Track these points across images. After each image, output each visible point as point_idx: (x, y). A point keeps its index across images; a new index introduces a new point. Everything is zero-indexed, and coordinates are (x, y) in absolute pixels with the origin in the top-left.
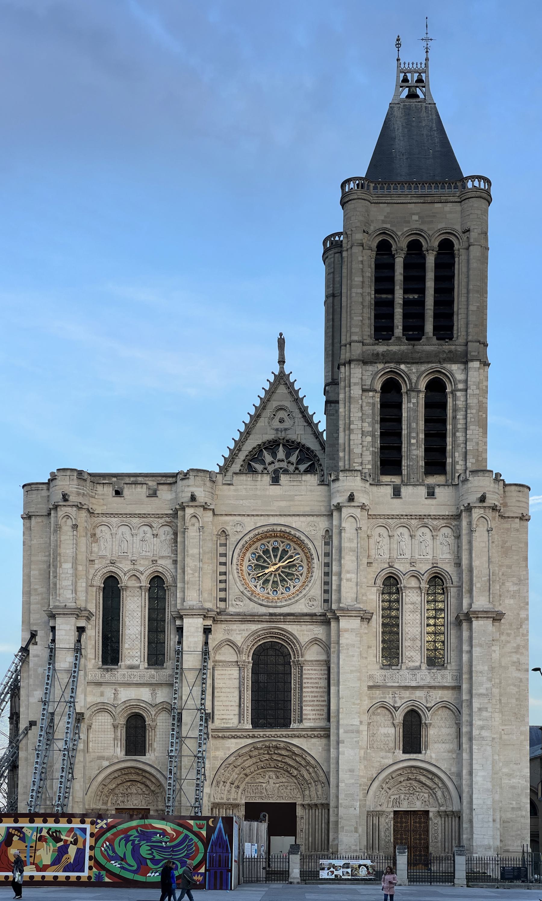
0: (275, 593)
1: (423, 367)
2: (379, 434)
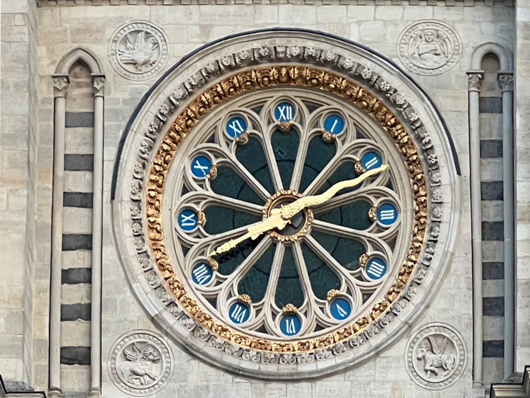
0: (291, 324)
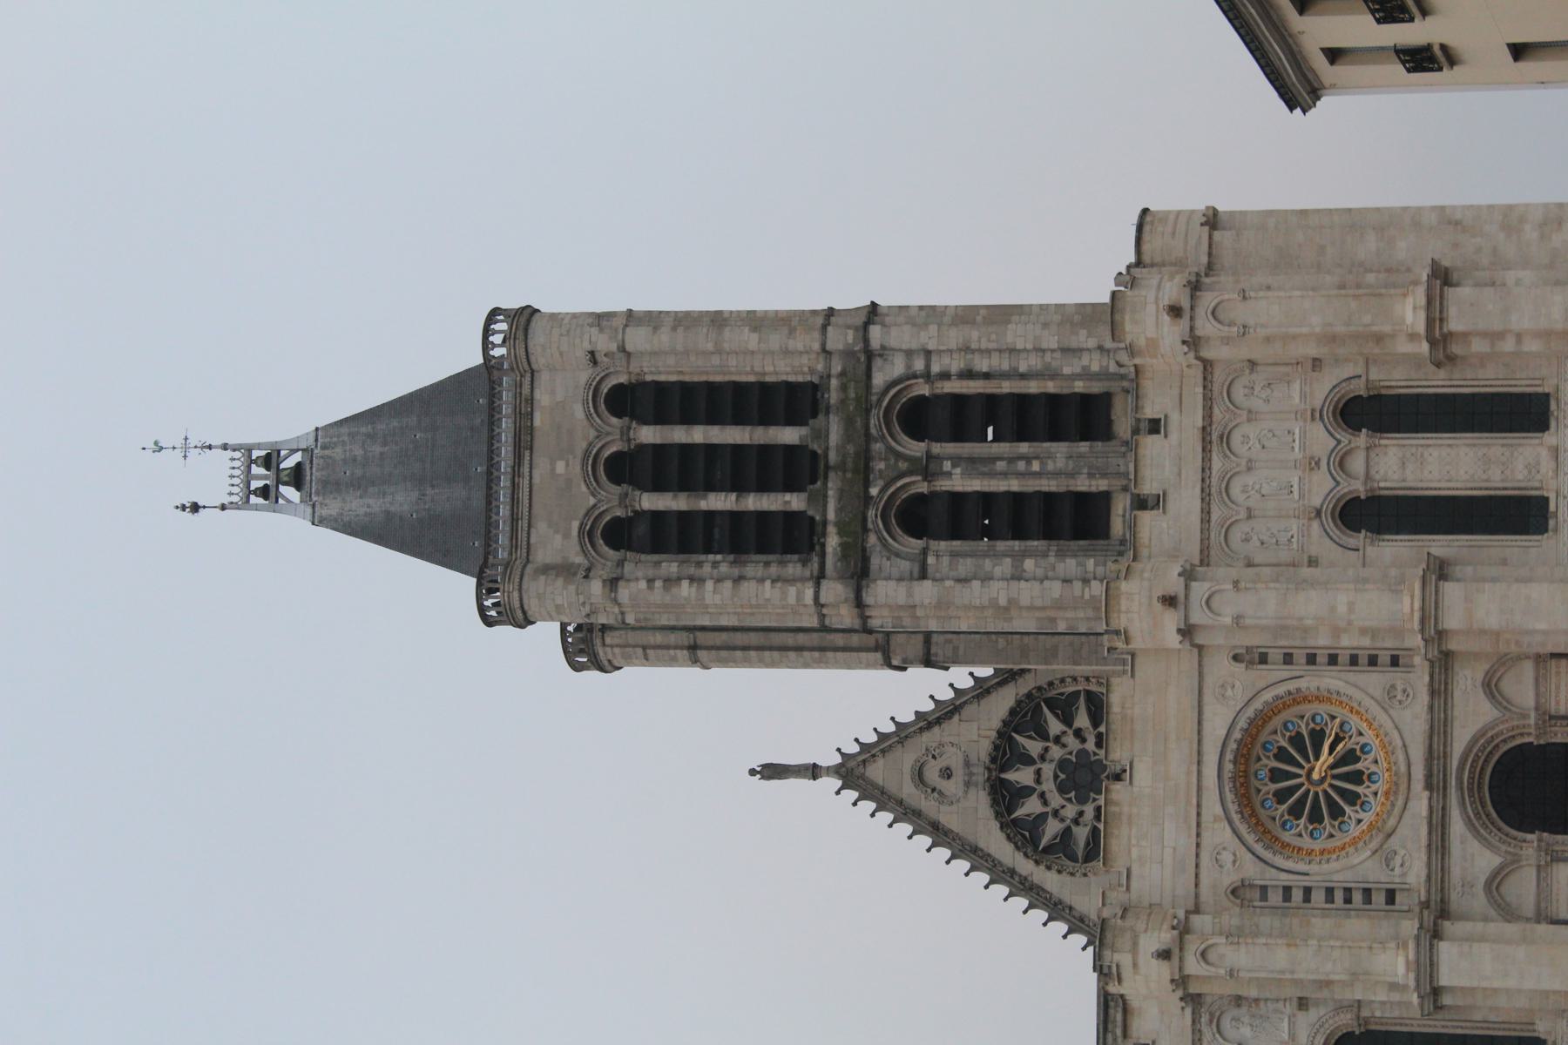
0: (1374, 778)
1: (877, 447)
2: (1017, 543)
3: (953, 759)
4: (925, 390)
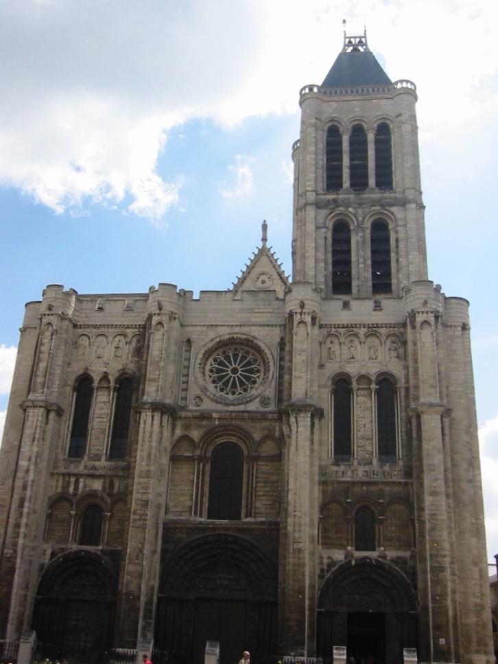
3: (268, 283)
4: (391, 226)
